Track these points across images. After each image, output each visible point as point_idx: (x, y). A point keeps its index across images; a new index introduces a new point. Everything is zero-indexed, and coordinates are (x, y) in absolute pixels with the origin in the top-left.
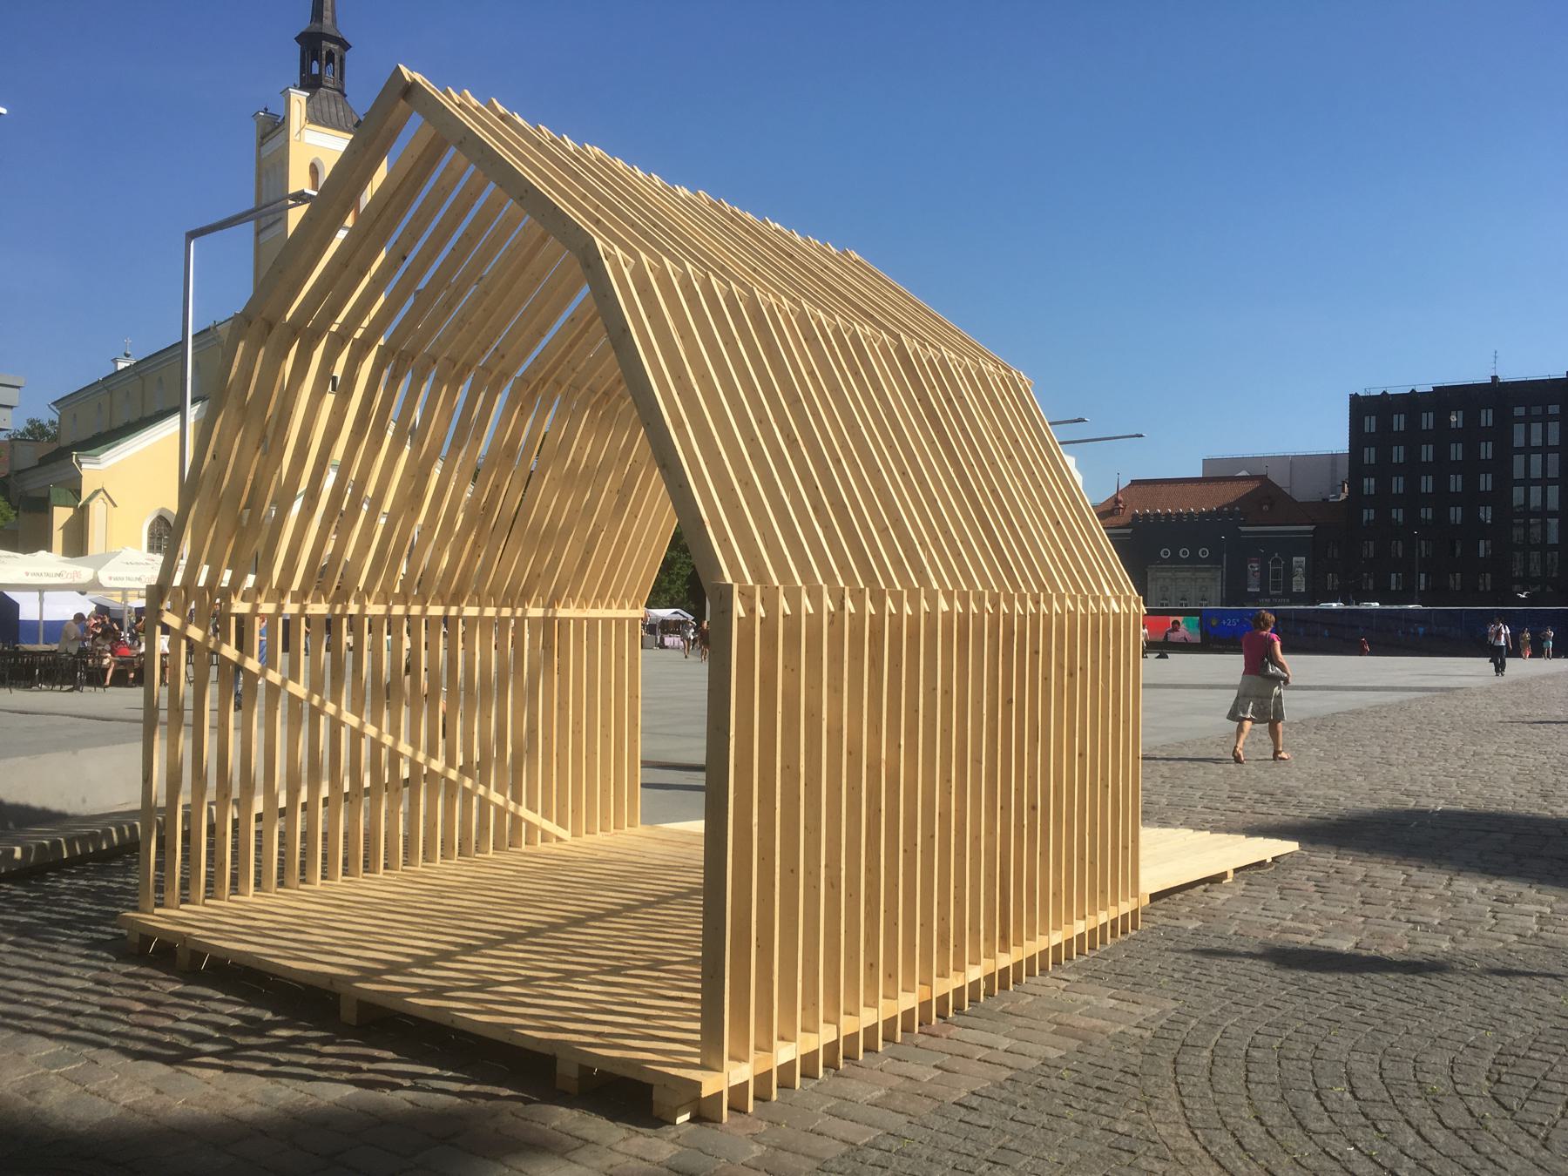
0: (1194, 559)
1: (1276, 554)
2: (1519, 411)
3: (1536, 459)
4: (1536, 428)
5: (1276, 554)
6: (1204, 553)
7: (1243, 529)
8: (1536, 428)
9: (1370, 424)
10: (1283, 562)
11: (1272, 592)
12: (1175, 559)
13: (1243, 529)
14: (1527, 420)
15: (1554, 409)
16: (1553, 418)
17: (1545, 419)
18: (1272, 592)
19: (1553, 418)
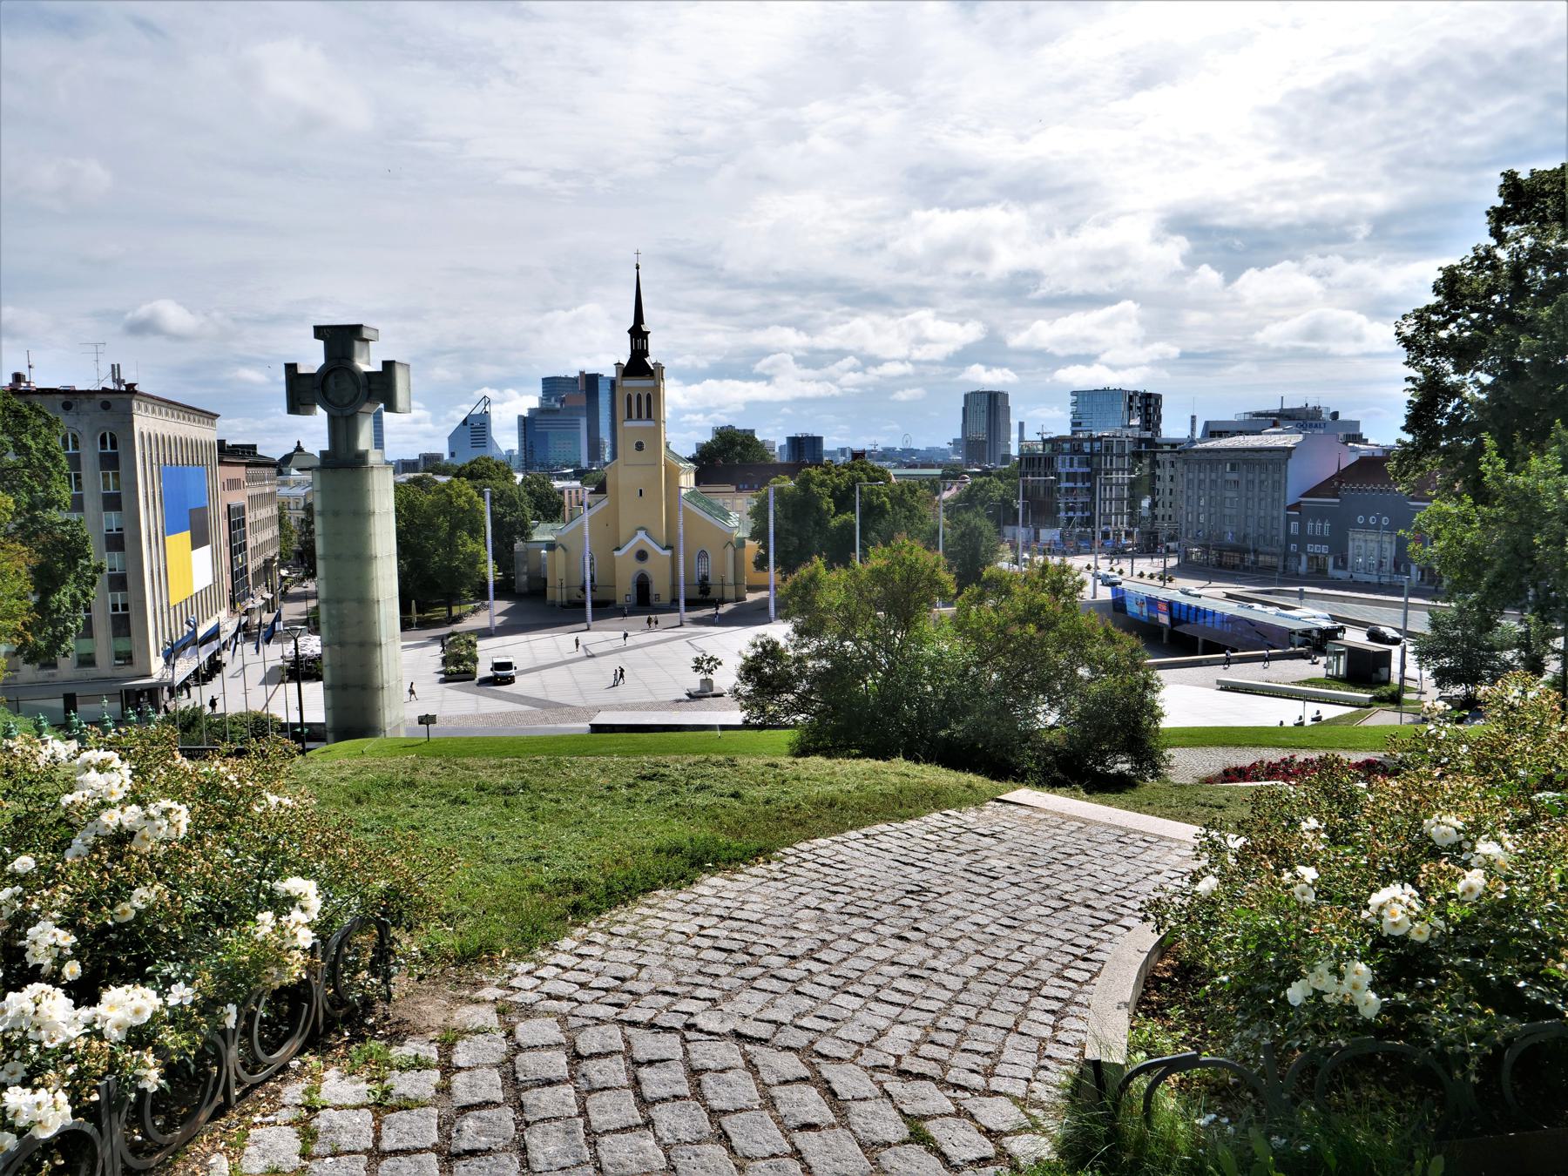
0: (1377, 527)
12: (1366, 526)
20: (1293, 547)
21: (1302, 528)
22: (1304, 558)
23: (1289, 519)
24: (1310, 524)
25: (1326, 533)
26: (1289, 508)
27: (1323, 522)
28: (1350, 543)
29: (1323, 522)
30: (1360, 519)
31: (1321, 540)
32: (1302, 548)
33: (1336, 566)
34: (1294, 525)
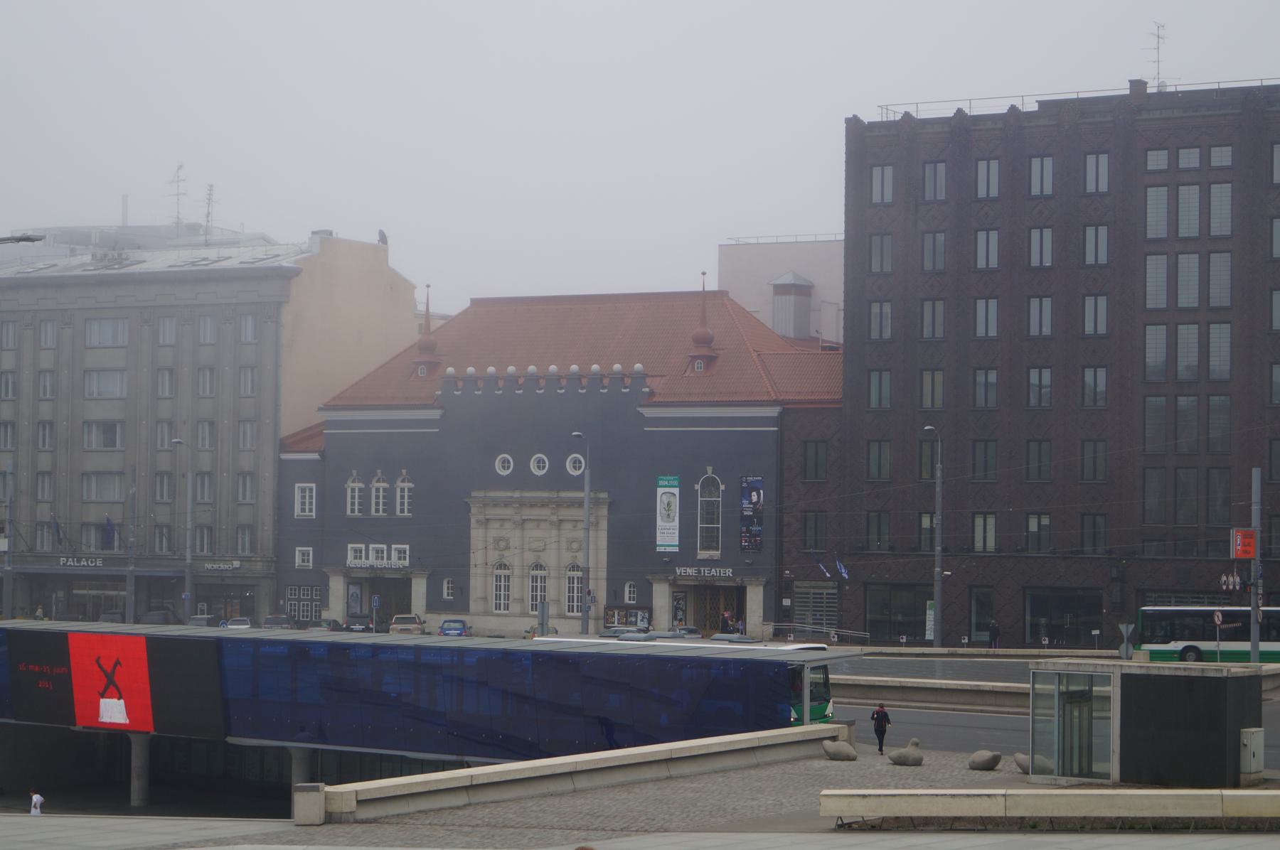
0: (557, 479)
1: (710, 469)
2: (1157, 160)
3: (1189, 264)
4: (1190, 196)
5: (710, 469)
6: (575, 464)
7: (649, 412)
8: (1190, 196)
9: (883, 185)
10: (722, 487)
11: (703, 555)
12: (521, 479)
13: (649, 412)
14: (1173, 179)
15: (1222, 157)
16: (1221, 175)
17: (1206, 177)
18: (703, 555)
19: (1221, 175)
20: (303, 556)
21: (330, 498)
22: (337, 586)
23: (285, 476)
24: (353, 486)
25: (403, 510)
26: (285, 445)
27: (391, 478)
28: (477, 534)
29: (391, 478)
30: (502, 466)
31: (386, 531)
32: (329, 555)
33: (434, 604)
34: (304, 500)
